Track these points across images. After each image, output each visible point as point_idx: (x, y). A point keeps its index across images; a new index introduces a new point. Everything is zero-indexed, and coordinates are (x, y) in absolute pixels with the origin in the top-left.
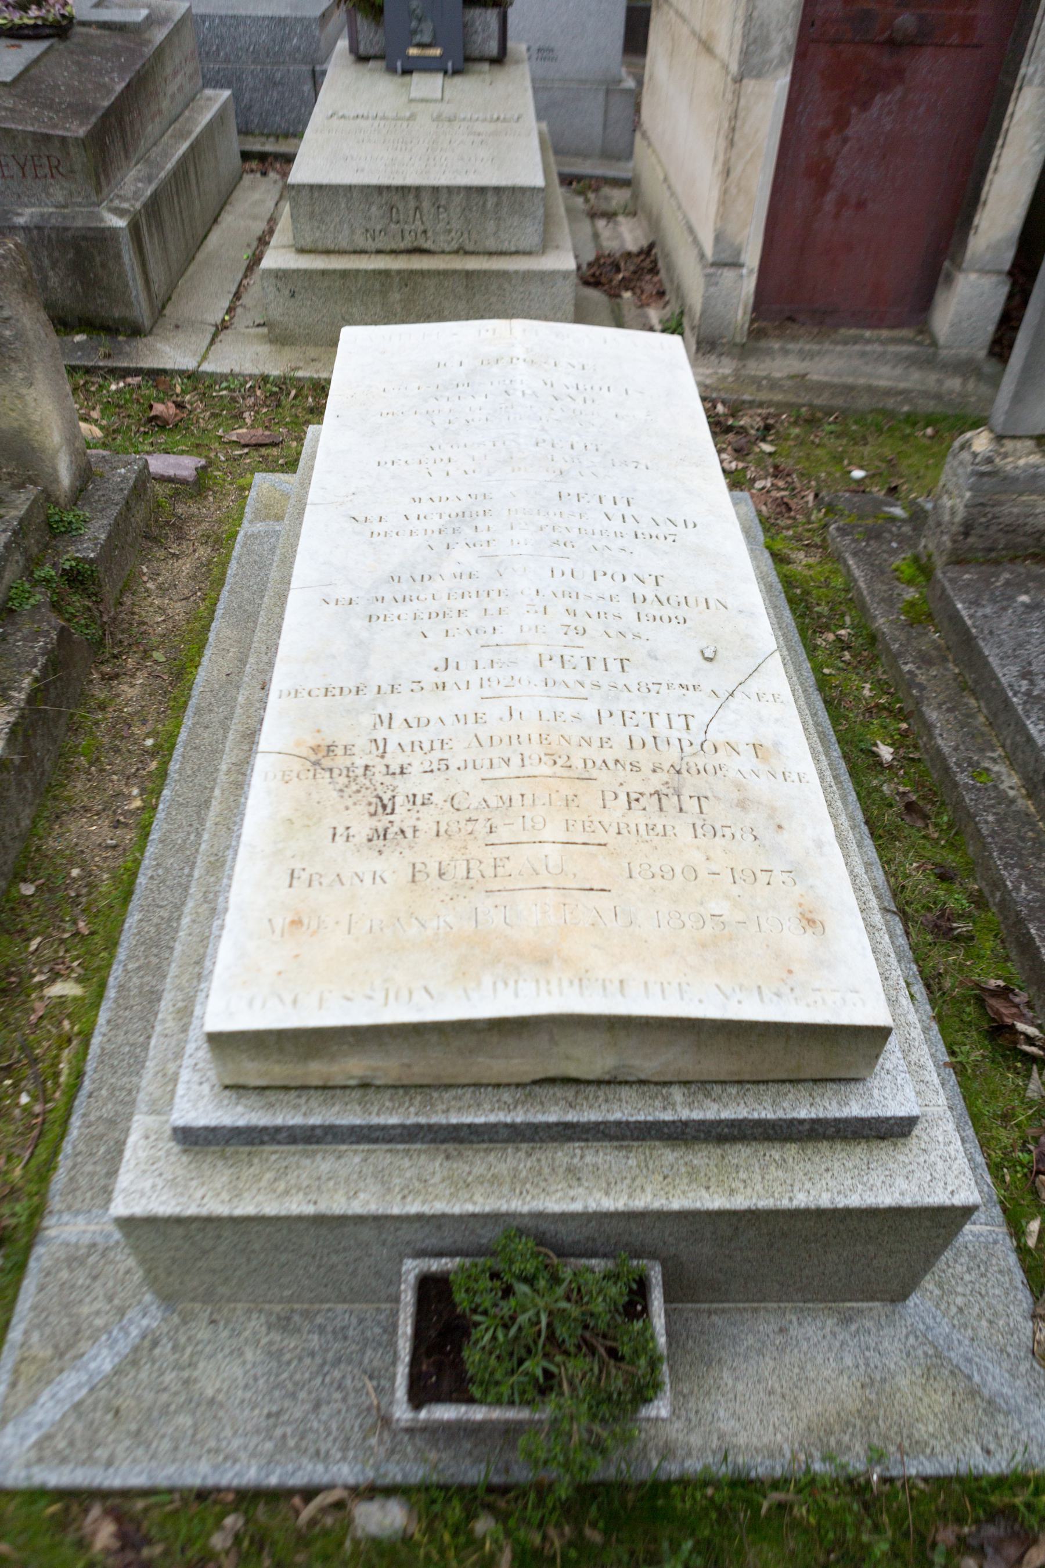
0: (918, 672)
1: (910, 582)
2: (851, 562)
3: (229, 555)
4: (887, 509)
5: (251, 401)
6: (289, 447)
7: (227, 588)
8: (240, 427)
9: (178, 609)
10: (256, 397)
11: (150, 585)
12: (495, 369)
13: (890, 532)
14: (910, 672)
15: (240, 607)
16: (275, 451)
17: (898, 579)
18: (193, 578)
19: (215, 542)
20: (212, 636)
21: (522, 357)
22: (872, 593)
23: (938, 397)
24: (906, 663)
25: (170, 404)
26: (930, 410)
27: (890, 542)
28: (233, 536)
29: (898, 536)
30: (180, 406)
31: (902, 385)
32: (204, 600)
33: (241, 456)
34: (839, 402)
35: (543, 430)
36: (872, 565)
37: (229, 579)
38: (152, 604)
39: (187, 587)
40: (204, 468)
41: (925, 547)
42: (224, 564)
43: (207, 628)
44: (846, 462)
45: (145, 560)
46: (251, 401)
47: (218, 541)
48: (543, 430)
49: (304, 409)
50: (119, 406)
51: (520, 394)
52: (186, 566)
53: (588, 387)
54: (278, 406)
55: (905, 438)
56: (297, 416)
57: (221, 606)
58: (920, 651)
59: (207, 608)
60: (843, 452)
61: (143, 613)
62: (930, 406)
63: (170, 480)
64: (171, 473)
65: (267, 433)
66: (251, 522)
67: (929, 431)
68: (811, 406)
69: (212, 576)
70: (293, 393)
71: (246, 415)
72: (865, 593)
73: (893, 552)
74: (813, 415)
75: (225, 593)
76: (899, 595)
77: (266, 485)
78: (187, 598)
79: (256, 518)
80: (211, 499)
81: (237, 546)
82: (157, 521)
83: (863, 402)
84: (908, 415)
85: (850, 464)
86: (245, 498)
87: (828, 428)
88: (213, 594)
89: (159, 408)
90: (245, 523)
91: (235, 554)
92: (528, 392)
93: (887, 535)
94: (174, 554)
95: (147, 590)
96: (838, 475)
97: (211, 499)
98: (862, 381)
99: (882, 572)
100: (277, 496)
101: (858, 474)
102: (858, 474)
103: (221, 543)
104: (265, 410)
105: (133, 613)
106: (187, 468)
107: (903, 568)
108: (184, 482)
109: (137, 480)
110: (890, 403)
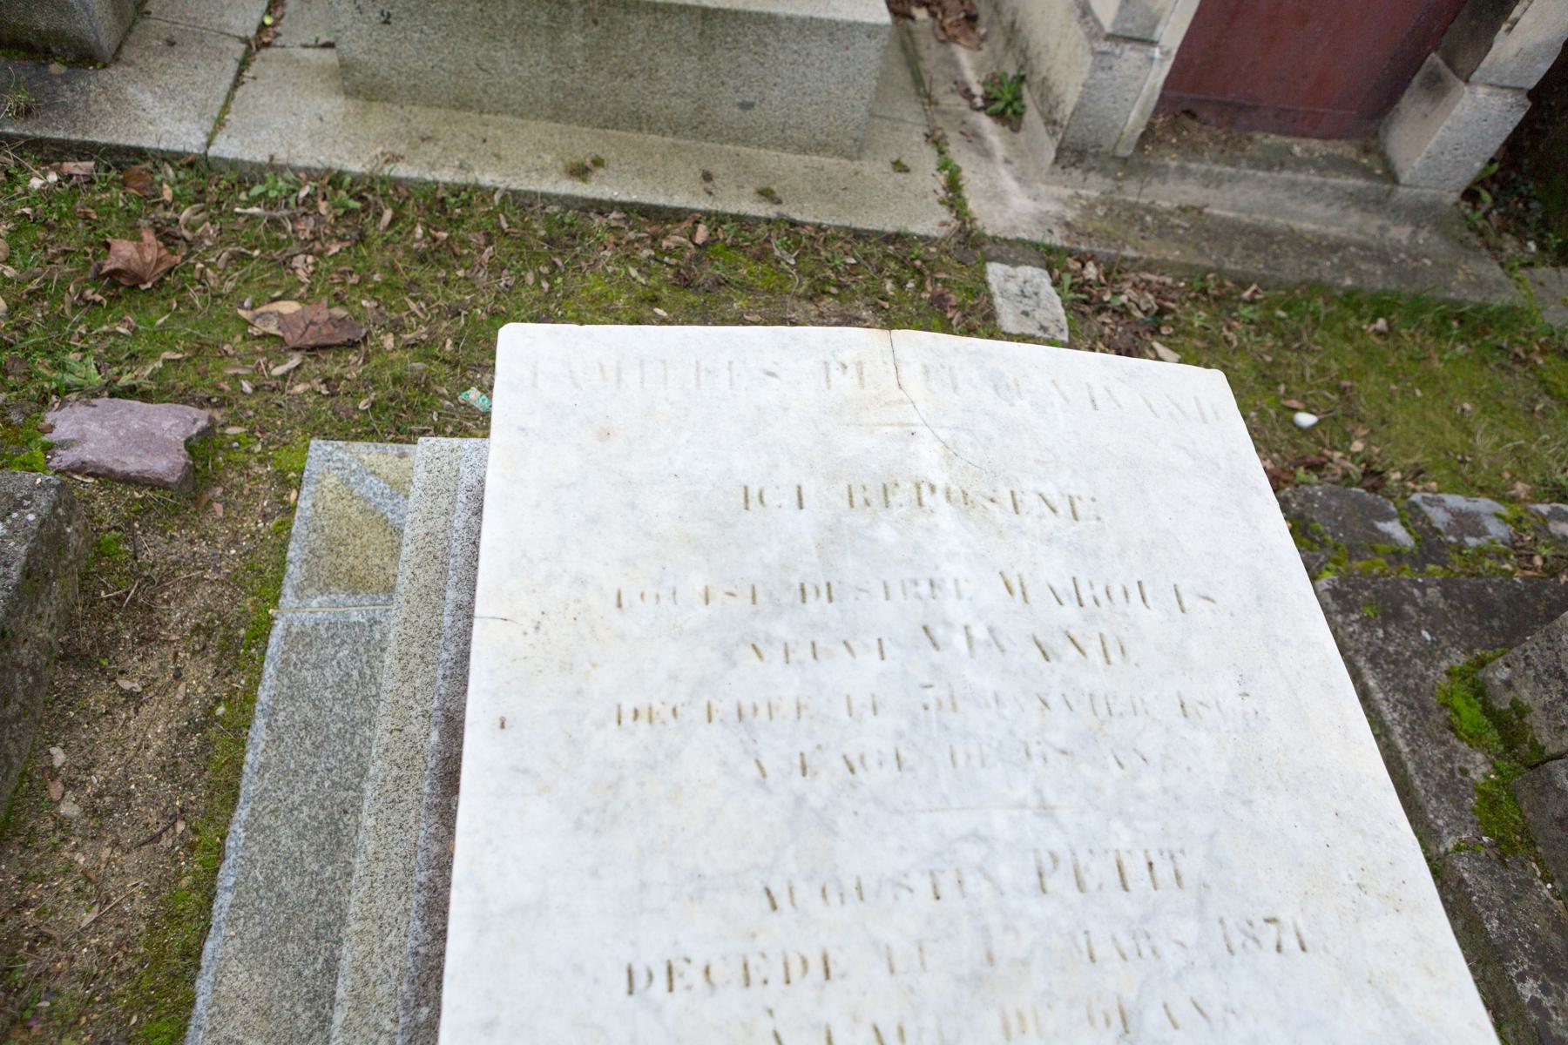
0: (1547, 1002)
1: (1474, 739)
2: (1372, 683)
3: (250, 697)
4: (1381, 526)
5: (306, 227)
6: (379, 350)
7: (242, 813)
8: (285, 297)
9: (131, 879)
10: (320, 219)
11: (69, 809)
12: (886, 533)
13: (1415, 604)
14: (1535, 1002)
15: (271, 883)
16: (353, 366)
17: (1452, 728)
18: (169, 770)
19: (223, 650)
20: (203, 985)
21: (940, 480)
22: (1420, 766)
23: (1382, 257)
24: (1522, 977)
25: (148, 236)
26: (1380, 286)
27: (1418, 626)
28: (261, 633)
29: (1426, 611)
30: (167, 236)
31: (1333, 231)
32: (192, 847)
33: (284, 377)
34: (1257, 266)
35: (1045, 809)
36: (1405, 690)
37: (249, 786)
38: (70, 867)
39: (152, 800)
40: (206, 434)
41: (1508, 684)
42: (238, 731)
43: (192, 954)
44: (1282, 388)
45: (60, 728)
46: (306, 227)
47: (230, 646)
48: (1045, 809)
49: (408, 250)
50: (50, 228)
51: (959, 640)
52: (154, 728)
53: (1100, 592)
54: (362, 238)
55: (1348, 337)
56: (394, 270)
57: (227, 877)
58: (1534, 934)
59: (196, 886)
60: (1273, 364)
61: (49, 901)
62: (1377, 279)
63: (129, 480)
64: (132, 464)
65: (339, 312)
66: (299, 590)
67: (1381, 323)
68: (1220, 272)
69: (210, 758)
70: (388, 215)
71: (298, 262)
72: (1411, 766)
73: (1429, 654)
74: (1221, 286)
75: (237, 833)
76: (1464, 772)
77: (331, 481)
78: (155, 838)
79: (310, 579)
80: (218, 507)
81: (269, 670)
82: (93, 601)
83: (1292, 269)
84: (1349, 293)
85: (1289, 394)
86: (290, 510)
87: (1245, 311)
88: (210, 833)
89: (124, 252)
90: (288, 599)
91: (263, 695)
92: (979, 633)
93: (1408, 608)
94: (129, 694)
95: (62, 824)
96: (1272, 412)
97: (218, 507)
98: (1279, 221)
99: (1426, 711)
100: (353, 512)
101: (1306, 419)
102: (1306, 419)
103: (236, 645)
104: (335, 249)
105: (26, 904)
106: (165, 447)
107: (1459, 702)
108: (156, 484)
109: (31, 554)
110: (1325, 268)
